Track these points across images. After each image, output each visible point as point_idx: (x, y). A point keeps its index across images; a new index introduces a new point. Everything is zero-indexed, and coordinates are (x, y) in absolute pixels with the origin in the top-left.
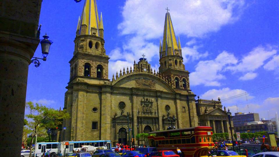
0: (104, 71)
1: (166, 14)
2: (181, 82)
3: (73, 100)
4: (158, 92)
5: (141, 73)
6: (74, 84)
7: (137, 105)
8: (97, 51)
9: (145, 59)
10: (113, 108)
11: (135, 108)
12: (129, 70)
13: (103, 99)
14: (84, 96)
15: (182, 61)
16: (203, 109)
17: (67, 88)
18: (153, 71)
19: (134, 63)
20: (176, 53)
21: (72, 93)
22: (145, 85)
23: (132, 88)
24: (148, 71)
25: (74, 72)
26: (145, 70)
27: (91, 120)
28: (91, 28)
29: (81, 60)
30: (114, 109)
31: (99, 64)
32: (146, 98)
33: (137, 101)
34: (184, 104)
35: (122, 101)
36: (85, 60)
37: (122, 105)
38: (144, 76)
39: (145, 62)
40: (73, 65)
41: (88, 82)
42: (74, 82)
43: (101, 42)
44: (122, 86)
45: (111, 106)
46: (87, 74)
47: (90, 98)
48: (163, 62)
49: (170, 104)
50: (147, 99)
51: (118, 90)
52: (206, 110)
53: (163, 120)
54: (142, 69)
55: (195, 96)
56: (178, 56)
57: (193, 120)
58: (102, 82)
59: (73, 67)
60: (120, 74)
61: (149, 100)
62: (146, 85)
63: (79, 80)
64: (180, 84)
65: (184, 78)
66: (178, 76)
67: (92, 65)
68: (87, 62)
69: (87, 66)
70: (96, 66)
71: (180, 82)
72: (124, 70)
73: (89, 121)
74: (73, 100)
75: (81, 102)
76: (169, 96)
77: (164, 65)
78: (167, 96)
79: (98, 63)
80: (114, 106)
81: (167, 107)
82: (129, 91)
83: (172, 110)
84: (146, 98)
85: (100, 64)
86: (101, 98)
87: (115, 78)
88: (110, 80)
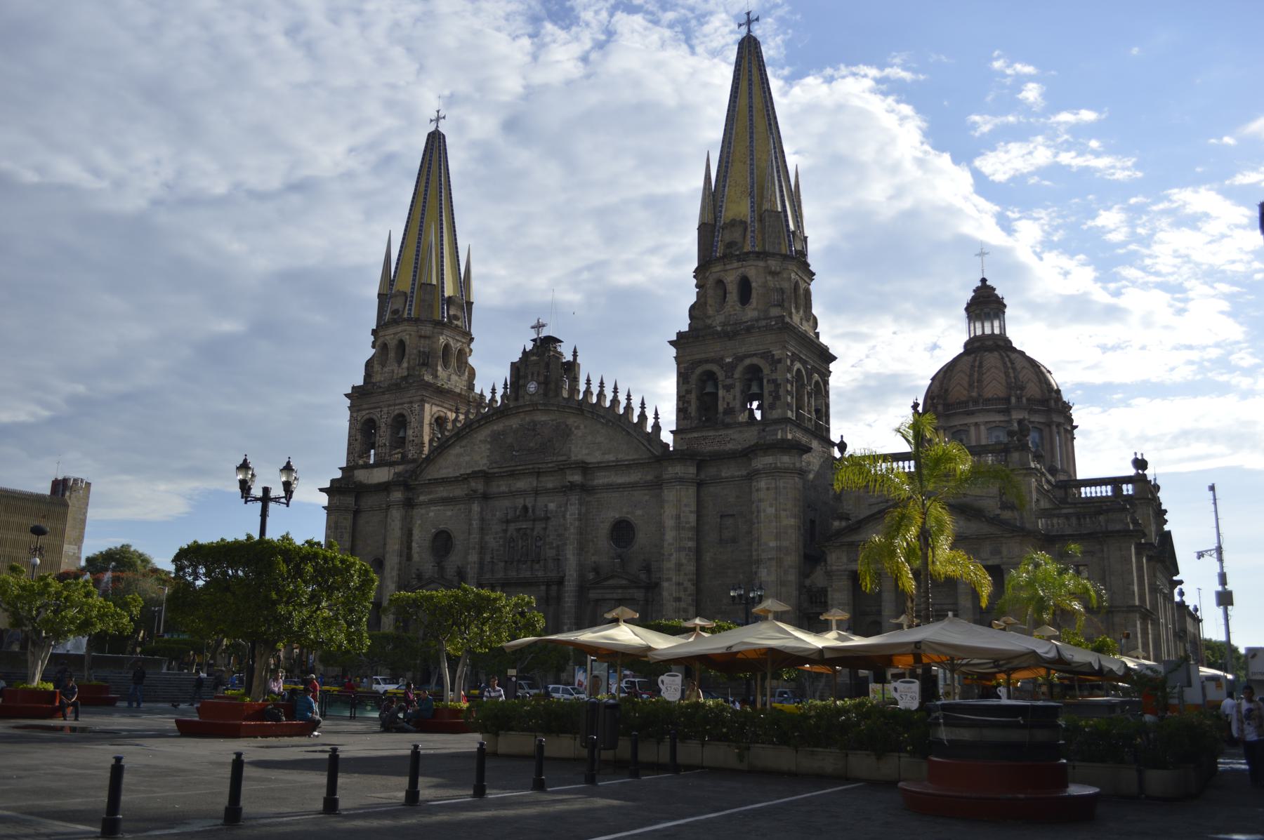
0: (410, 432)
2: (728, 388)
4: (568, 472)
7: (487, 538)
10: (416, 557)
24: (541, 391)
32: (520, 502)
33: (482, 520)
38: (522, 415)
44: (444, 473)
45: (409, 548)
49: (639, 512)
65: (748, 362)
71: (721, 393)
76: (634, 477)
81: (622, 531)
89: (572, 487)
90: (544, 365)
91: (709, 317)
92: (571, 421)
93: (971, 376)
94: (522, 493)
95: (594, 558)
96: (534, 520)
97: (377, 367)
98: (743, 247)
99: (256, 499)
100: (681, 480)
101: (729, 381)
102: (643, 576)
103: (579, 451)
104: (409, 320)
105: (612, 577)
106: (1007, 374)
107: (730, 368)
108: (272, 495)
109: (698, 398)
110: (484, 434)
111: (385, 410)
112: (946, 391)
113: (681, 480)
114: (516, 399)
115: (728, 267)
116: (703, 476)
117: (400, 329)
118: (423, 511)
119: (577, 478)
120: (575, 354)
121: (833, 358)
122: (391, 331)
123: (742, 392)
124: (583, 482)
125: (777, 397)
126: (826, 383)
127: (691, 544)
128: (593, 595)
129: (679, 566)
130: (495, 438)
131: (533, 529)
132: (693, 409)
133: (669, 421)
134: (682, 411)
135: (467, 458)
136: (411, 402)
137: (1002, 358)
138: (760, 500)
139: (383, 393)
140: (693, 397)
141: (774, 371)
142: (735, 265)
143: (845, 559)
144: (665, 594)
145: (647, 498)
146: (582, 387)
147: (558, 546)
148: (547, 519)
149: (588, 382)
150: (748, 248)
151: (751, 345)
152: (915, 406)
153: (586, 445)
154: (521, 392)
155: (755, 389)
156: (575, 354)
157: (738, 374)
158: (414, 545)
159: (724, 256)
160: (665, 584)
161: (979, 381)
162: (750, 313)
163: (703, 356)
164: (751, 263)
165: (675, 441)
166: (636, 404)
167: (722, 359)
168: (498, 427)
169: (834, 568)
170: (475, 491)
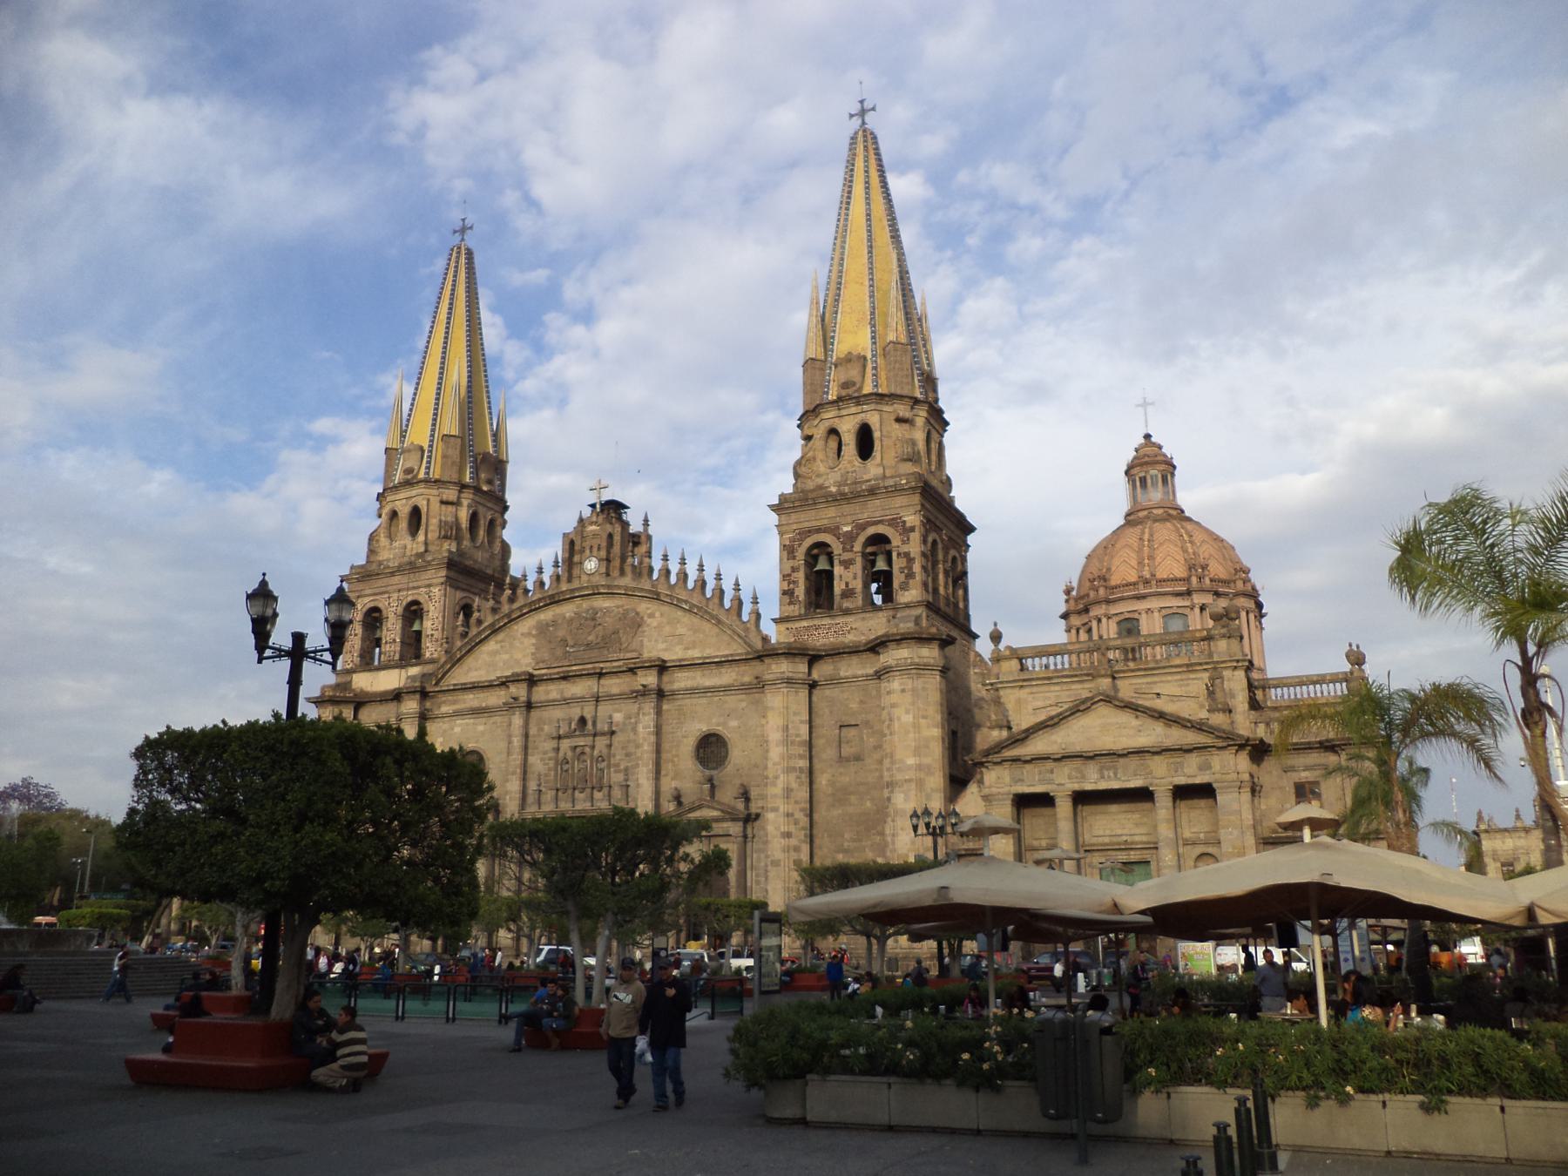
2: (847, 564)
4: (639, 672)
5: (564, 587)
11: (514, 773)
24: (603, 570)
32: (575, 712)
34: (854, 706)
36: (366, 600)
41: (369, 689)
49: (733, 723)
51: (455, 702)
57: (891, 810)
64: (836, 583)
65: (871, 531)
70: (400, 610)
76: (727, 676)
78: (708, 682)
81: (711, 748)
83: (738, 754)
89: (644, 692)
90: (612, 533)
91: (819, 476)
92: (644, 607)
93: (1140, 551)
94: (580, 700)
95: (674, 784)
96: (595, 735)
97: (384, 541)
98: (861, 388)
99: (280, 653)
100: (789, 682)
101: (847, 556)
102: (740, 805)
103: (654, 646)
104: (427, 481)
105: (700, 807)
106: (1185, 551)
108: (309, 645)
109: (807, 578)
110: (527, 624)
111: (395, 596)
112: (1109, 570)
113: (789, 682)
114: (569, 580)
115: (844, 412)
116: (815, 676)
117: (414, 492)
118: (446, 726)
119: (650, 679)
120: (646, 522)
121: (971, 529)
122: (403, 494)
123: (864, 568)
124: (659, 684)
125: (910, 575)
126: (964, 559)
127: (804, 763)
129: (788, 792)
130: (543, 629)
131: (593, 747)
132: (800, 592)
133: (771, 608)
134: (788, 593)
135: (506, 657)
136: (429, 586)
137: (1177, 530)
138: (893, 706)
139: (392, 574)
140: (800, 576)
141: (906, 541)
142: (853, 410)
143: (1007, 779)
144: (770, 828)
145: (744, 704)
146: (657, 564)
147: (626, 769)
148: (613, 733)
149: (665, 558)
150: (868, 389)
151: (873, 509)
152: (1068, 592)
153: (665, 635)
154: (576, 572)
155: (881, 565)
156: (646, 522)
157: (858, 547)
159: (840, 399)
160: (770, 816)
161: (1151, 557)
162: (872, 470)
164: (873, 406)
165: (779, 633)
166: (728, 586)
167: (838, 528)
168: (546, 615)
169: (994, 790)
170: (515, 699)
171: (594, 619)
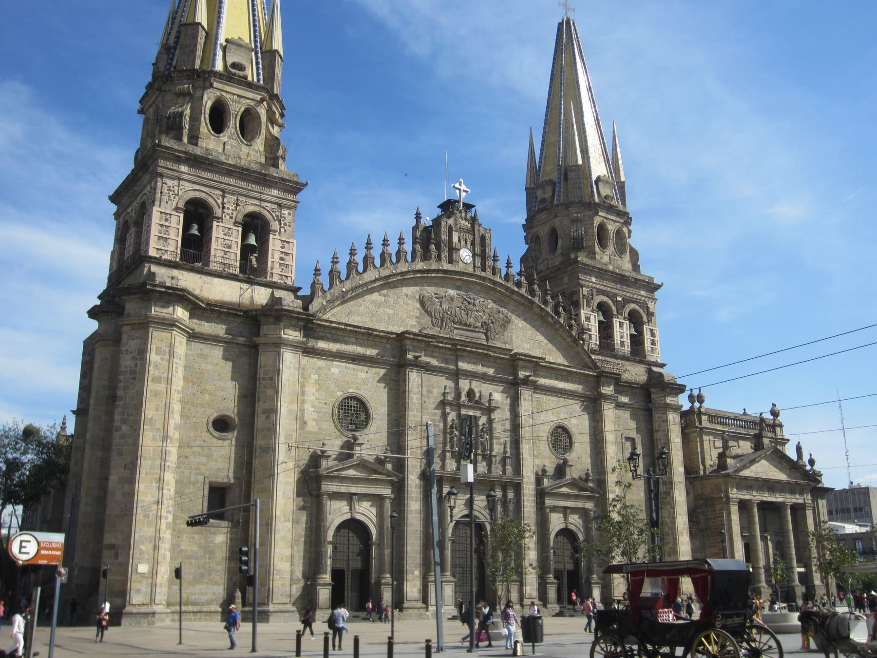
1: (560, 25)
3: (123, 369)
4: (520, 363)
5: (446, 266)
6: (129, 291)
8: (245, 149)
9: (468, 207)
10: (311, 426)
12: (393, 249)
13: (264, 379)
14: (172, 354)
15: (625, 230)
16: (711, 450)
17: (93, 313)
18: (501, 265)
19: (413, 223)
20: (603, 194)
21: (117, 340)
22: (465, 325)
23: (403, 333)
24: (478, 264)
25: (130, 240)
26: (465, 254)
27: (202, 474)
28: (227, 41)
29: (170, 182)
30: (316, 429)
31: (250, 209)
35: (352, 391)
37: (353, 412)
39: (466, 219)
40: (129, 210)
41: (197, 292)
42: (130, 281)
43: (269, 111)
44: (356, 320)
46: (195, 251)
47: (203, 365)
48: (543, 231)
49: (574, 421)
50: (470, 393)
52: (722, 457)
53: (541, 494)
54: (452, 250)
55: (681, 389)
56: (611, 209)
58: (261, 296)
59: (127, 217)
60: (351, 266)
61: (480, 396)
62: (470, 326)
63: (152, 275)
65: (633, 306)
66: (612, 297)
67: (218, 212)
68: (197, 195)
69: (198, 215)
72: (369, 246)
73: (193, 479)
74: (123, 369)
75: (156, 380)
77: (545, 246)
79: (251, 207)
80: (315, 415)
82: (388, 346)
84: (465, 385)
85: (257, 209)
86: (256, 374)
87: (324, 279)
88: (299, 289)
89: (526, 382)
107: (620, 306)
111: (230, 199)
117: (250, 95)
118: (321, 363)
128: (549, 502)
158: (307, 407)
163: (603, 288)
171: (474, 305)
